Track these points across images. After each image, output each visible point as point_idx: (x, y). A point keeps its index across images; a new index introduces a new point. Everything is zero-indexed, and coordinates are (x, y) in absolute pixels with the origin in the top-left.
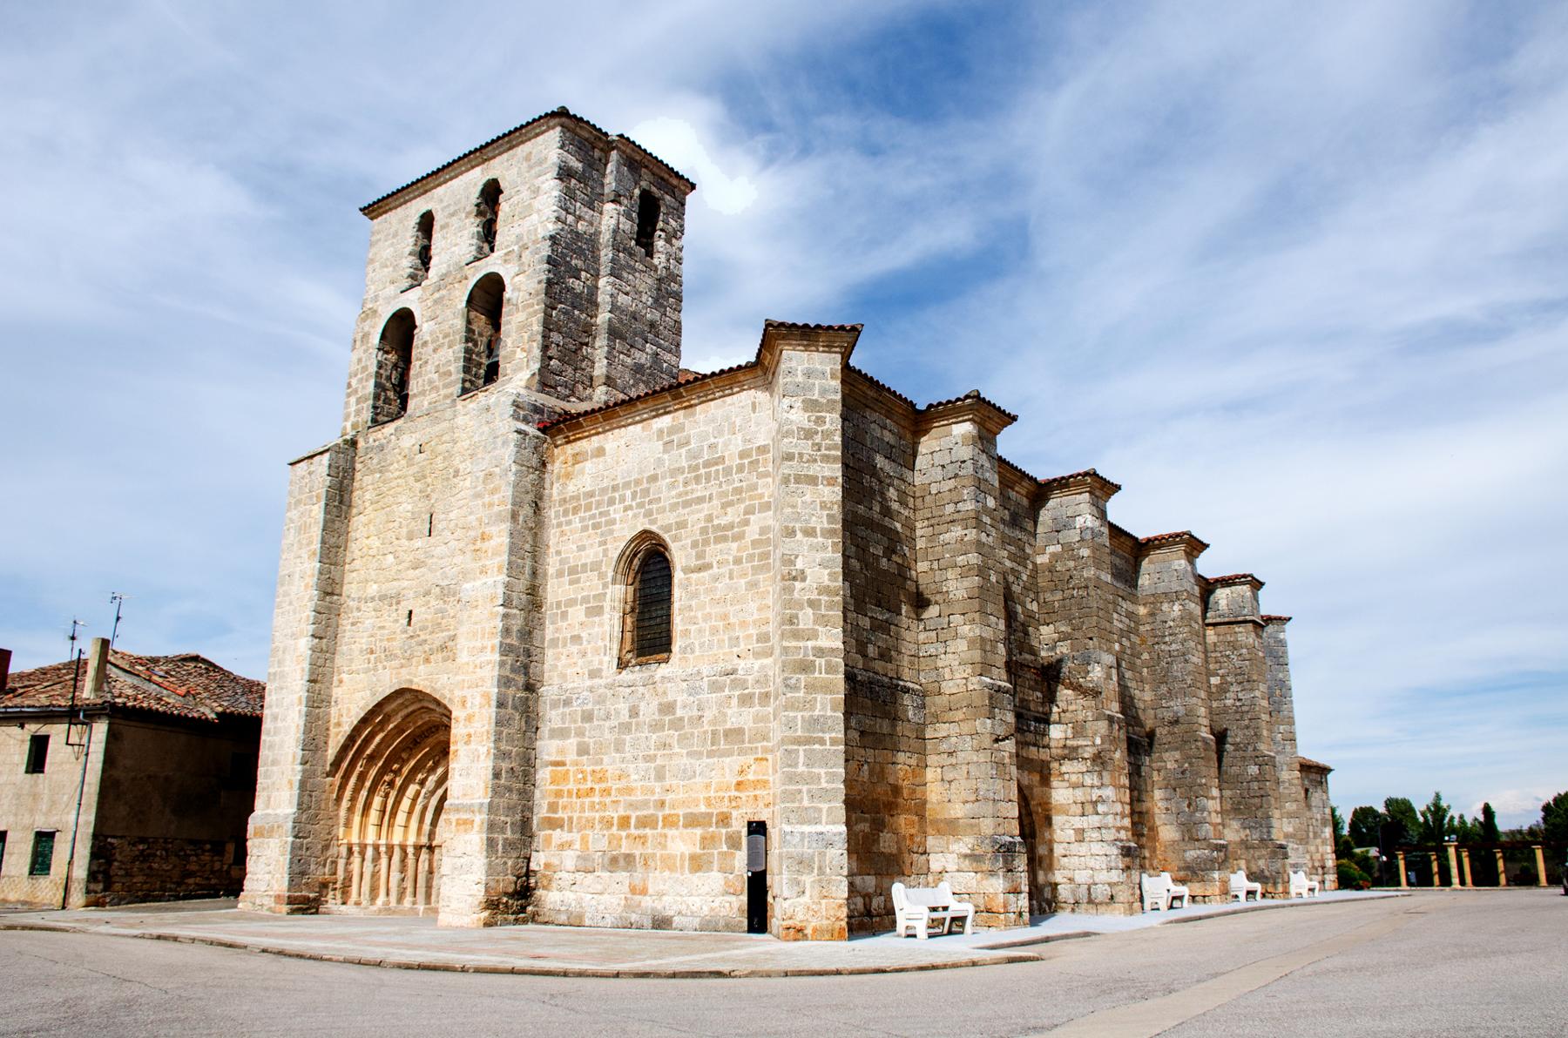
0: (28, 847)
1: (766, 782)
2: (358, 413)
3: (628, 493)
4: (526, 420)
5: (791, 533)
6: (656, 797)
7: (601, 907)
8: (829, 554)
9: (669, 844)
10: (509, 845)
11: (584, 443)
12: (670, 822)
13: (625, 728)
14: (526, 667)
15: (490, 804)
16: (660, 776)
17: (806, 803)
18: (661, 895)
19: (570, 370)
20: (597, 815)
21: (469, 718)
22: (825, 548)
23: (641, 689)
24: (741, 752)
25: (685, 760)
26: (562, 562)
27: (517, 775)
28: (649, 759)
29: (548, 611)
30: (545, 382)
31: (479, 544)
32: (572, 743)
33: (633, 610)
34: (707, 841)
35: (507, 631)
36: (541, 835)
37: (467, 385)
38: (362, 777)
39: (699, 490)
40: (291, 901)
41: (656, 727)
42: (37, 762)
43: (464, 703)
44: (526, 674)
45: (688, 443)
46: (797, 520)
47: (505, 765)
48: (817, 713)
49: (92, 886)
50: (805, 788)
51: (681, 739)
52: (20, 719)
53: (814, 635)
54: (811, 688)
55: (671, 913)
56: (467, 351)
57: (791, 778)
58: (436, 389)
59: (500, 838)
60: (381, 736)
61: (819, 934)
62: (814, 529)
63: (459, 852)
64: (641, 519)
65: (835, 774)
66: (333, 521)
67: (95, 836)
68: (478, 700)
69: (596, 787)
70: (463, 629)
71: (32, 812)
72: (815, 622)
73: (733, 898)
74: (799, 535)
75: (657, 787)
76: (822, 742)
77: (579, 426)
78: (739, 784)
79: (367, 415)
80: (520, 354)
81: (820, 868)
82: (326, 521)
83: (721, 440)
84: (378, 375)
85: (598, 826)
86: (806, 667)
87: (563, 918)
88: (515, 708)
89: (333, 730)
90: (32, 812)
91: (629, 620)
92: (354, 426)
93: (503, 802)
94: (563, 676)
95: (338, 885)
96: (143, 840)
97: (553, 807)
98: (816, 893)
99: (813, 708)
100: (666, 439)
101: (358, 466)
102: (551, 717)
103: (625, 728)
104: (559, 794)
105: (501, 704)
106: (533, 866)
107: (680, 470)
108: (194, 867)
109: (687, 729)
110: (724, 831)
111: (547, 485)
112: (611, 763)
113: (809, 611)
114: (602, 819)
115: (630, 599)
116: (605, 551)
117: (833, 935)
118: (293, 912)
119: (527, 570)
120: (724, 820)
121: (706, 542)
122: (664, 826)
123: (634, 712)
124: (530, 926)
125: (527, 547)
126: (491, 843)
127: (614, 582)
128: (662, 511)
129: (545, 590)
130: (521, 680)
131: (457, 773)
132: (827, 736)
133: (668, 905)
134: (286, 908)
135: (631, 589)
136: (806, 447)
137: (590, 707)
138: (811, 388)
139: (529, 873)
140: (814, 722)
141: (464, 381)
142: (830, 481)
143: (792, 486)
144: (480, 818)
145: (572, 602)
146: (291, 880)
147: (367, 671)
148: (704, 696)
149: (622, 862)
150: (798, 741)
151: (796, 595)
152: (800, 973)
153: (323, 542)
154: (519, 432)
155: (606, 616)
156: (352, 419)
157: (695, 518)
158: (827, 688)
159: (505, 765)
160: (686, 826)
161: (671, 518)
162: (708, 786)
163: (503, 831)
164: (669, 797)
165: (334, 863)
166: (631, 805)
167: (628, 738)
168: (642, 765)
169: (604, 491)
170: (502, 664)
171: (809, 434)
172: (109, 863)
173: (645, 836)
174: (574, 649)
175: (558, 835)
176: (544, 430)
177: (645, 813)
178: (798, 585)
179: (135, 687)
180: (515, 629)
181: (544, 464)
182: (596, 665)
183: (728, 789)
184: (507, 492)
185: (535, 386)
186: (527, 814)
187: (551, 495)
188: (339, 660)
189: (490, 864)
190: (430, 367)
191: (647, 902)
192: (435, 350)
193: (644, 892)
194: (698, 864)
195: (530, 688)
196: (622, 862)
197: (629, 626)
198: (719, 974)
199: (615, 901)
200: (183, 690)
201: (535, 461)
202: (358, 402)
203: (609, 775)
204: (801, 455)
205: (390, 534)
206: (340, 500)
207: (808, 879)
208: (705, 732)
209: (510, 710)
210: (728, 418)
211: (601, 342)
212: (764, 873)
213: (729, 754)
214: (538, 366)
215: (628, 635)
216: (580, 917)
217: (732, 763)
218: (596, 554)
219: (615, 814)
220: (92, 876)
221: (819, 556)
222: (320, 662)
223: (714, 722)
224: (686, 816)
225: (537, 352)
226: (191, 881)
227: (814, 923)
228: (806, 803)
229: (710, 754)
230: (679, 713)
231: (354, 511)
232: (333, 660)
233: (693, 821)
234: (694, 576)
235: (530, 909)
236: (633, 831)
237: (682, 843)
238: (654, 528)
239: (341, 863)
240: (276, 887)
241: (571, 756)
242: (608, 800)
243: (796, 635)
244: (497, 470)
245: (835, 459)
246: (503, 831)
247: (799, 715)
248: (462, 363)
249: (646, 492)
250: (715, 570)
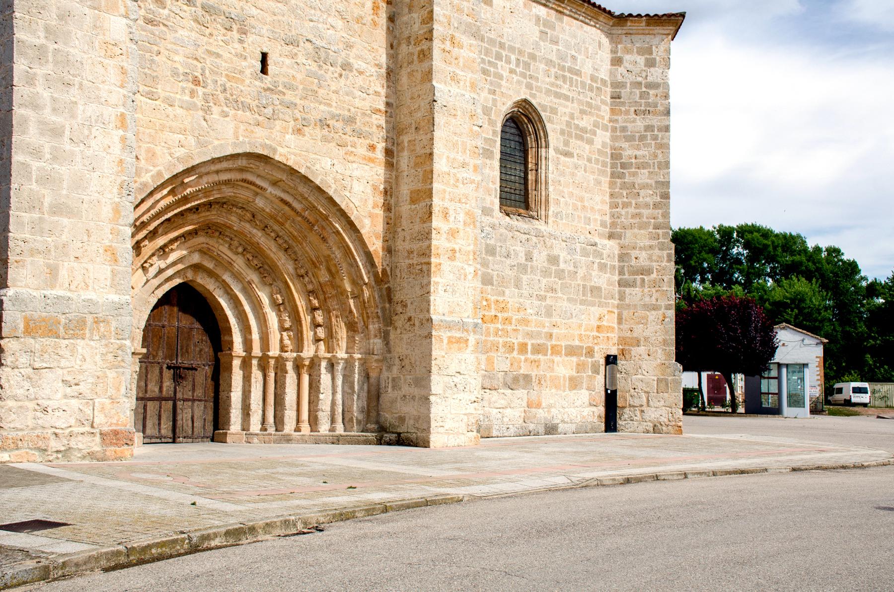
1: (613, 328)
12: (555, 350)
13: (523, 268)
16: (549, 314)
18: (550, 406)
20: (501, 340)
23: (534, 239)
24: (600, 305)
25: (565, 304)
31: (448, 46)
34: (580, 367)
41: (546, 273)
43: (446, 215)
51: (564, 286)
55: (556, 421)
63: (452, 370)
68: (462, 217)
69: (499, 315)
73: (594, 409)
75: (547, 321)
78: (598, 327)
85: (502, 350)
103: (523, 268)
110: (590, 360)
112: (511, 296)
114: (505, 344)
116: (494, 100)
120: (590, 352)
122: (552, 354)
123: (529, 258)
131: (441, 288)
133: (556, 415)
137: (492, 242)
147: (190, 107)
149: (522, 382)
160: (566, 355)
162: (580, 326)
164: (555, 331)
166: (530, 335)
173: (539, 361)
177: (539, 342)
183: (592, 330)
191: (541, 414)
193: (539, 406)
194: (574, 383)
196: (522, 382)
199: (517, 414)
203: (509, 306)
208: (579, 285)
212: (614, 392)
213: (594, 305)
217: (596, 311)
223: (584, 278)
224: (567, 347)
229: (583, 303)
230: (562, 266)
233: (571, 351)
237: (564, 367)
240: (99, 419)
242: (509, 328)
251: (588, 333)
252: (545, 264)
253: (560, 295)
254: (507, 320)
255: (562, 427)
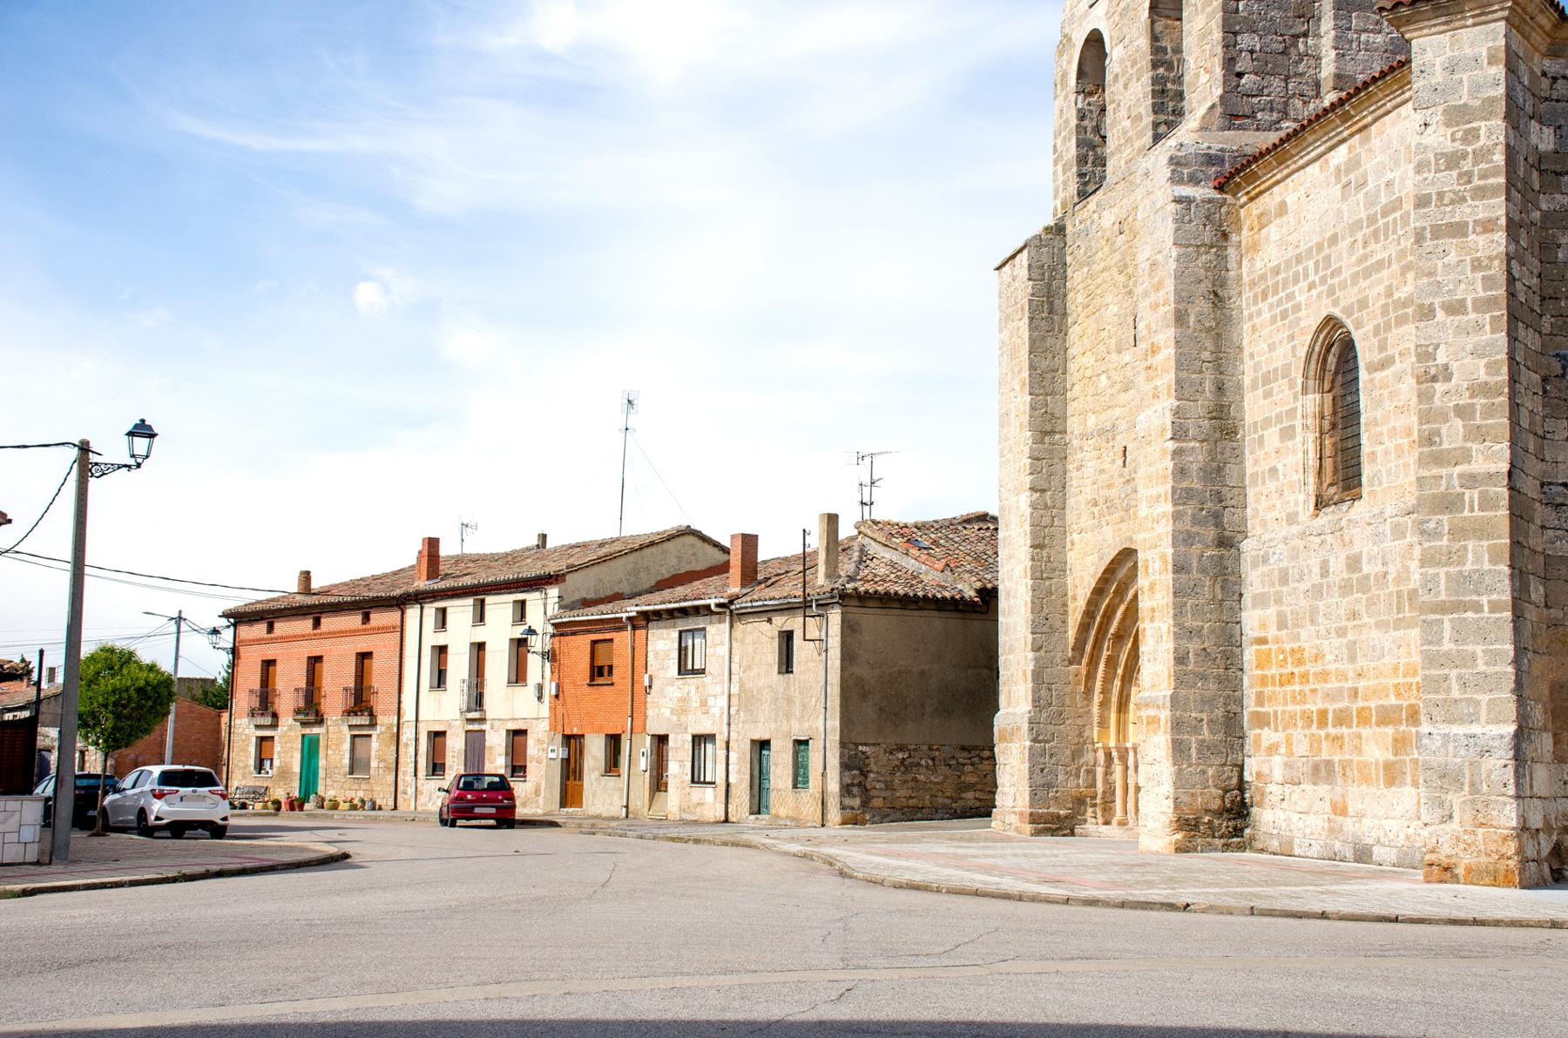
0: (787, 758)
2: (1065, 183)
3: (1311, 264)
4: (1194, 180)
5: (1426, 313)
6: (1350, 684)
7: (1308, 831)
8: (1487, 336)
9: (1365, 748)
10: (1206, 749)
11: (1265, 198)
13: (1317, 591)
14: (1217, 518)
15: (1174, 699)
16: (1352, 658)
17: (1456, 693)
19: (1277, 83)
21: (1152, 587)
22: (1479, 327)
23: (1330, 538)
25: (1374, 633)
26: (1256, 368)
27: (1216, 658)
28: (1341, 632)
29: (1248, 438)
30: (1233, 113)
32: (1272, 611)
33: (1334, 426)
35: (1181, 472)
36: (1251, 734)
37: (1162, 129)
38: (1112, 663)
39: (1379, 252)
40: (1034, 819)
41: (1346, 588)
42: (786, 664)
44: (1218, 524)
45: (1365, 184)
46: (1436, 295)
47: (1193, 646)
48: (1468, 567)
49: (848, 801)
50: (1454, 673)
51: (1371, 603)
52: (767, 613)
53: (1466, 456)
54: (1458, 532)
56: (1155, 81)
57: (1431, 660)
58: (1129, 141)
59: (1193, 741)
60: (1122, 608)
61: (1475, 876)
62: (1462, 302)
64: (1326, 301)
65: (1497, 653)
66: (1043, 338)
67: (843, 744)
70: (1141, 473)
71: (788, 716)
72: (1466, 438)
74: (1440, 315)
75: (1349, 668)
76: (1477, 608)
77: (1254, 177)
79: (1073, 188)
80: (1204, 78)
81: (1472, 784)
82: (1032, 342)
83: (1398, 173)
84: (1080, 129)
86: (1449, 503)
87: (1274, 844)
88: (1203, 571)
89: (1071, 605)
90: (788, 716)
91: (1328, 442)
92: (1064, 205)
93: (1192, 694)
94: (1264, 523)
95: (1098, 801)
96: (901, 749)
97: (1260, 699)
98: (1468, 817)
99: (1462, 561)
100: (1344, 180)
101: (1069, 259)
102: (1254, 580)
103: (1317, 591)
104: (1264, 680)
105: (1179, 568)
106: (1247, 777)
107: (1357, 225)
108: (971, 779)
109: (1374, 591)
111: (1232, 264)
112: (1308, 638)
113: (1458, 423)
115: (1327, 411)
117: (1496, 878)
118: (1038, 833)
119: (1208, 386)
121: (1388, 328)
123: (1325, 572)
124: (1248, 855)
125: (1206, 355)
126: (1179, 749)
127: (1305, 391)
128: (1343, 286)
129: (1241, 409)
130: (1210, 533)
132: (1484, 600)
134: (1028, 828)
135: (1328, 397)
136: (1449, 181)
137: (1284, 564)
138: (1455, 89)
139: (1241, 786)
140: (1460, 581)
141: (1156, 125)
142: (1487, 226)
143: (1428, 244)
144: (1165, 715)
145: (1267, 423)
146: (1033, 794)
148: (1388, 544)
149: (1323, 773)
150: (1442, 608)
151: (1437, 402)
152: (1270, 913)
153: (1032, 367)
154: (1178, 200)
155: (1299, 439)
156: (1061, 195)
157: (1374, 289)
158: (1481, 530)
159: (1193, 646)
160: (1378, 725)
161: (1349, 297)
162: (1396, 669)
163: (1196, 730)
164: (1362, 684)
165: (1091, 772)
166: (1328, 696)
167: (1321, 604)
168: (1336, 641)
169: (1288, 263)
170: (1177, 516)
171: (1453, 160)
172: (864, 774)
174: (1272, 485)
175: (1268, 736)
176: (1220, 188)
178: (1440, 387)
179: (892, 564)
180: (1195, 466)
181: (1225, 236)
182: (1292, 509)
184: (1169, 286)
185: (1217, 120)
186: (1233, 708)
187: (1239, 278)
188: (1070, 516)
189: (1179, 772)
190: (1123, 113)
192: (1125, 87)
193: (1343, 812)
195: (1226, 542)
197: (1328, 452)
198: (1172, 907)
200: (940, 565)
201: (1208, 235)
202: (1064, 172)
203: (1306, 654)
204: (1440, 195)
205: (1102, 347)
206: (1048, 308)
207: (1456, 799)
209: (1195, 574)
210: (1402, 139)
211: (1327, 25)
214: (1220, 91)
215: (1328, 463)
216: (1291, 843)
218: (1285, 356)
219: (1313, 707)
220: (846, 790)
221: (1470, 342)
222: (1046, 520)
223: (1398, 581)
225: (1219, 72)
226: (970, 795)
227: (1466, 860)
228: (1456, 693)
231: (1070, 320)
232: (1063, 518)
233: (1386, 717)
234: (1378, 375)
235: (1247, 831)
236: (1332, 730)
238: (1337, 312)
239: (1100, 771)
241: (1272, 632)
243: (1439, 459)
244: (1159, 257)
245: (1493, 191)
246: (1196, 730)
247: (1442, 571)
248: (1150, 102)
249: (1327, 259)
250: (1398, 366)
251: (1409, 679)
252: (1345, 575)
253: (1366, 620)
254: (1305, 677)
255: (1375, 849)
